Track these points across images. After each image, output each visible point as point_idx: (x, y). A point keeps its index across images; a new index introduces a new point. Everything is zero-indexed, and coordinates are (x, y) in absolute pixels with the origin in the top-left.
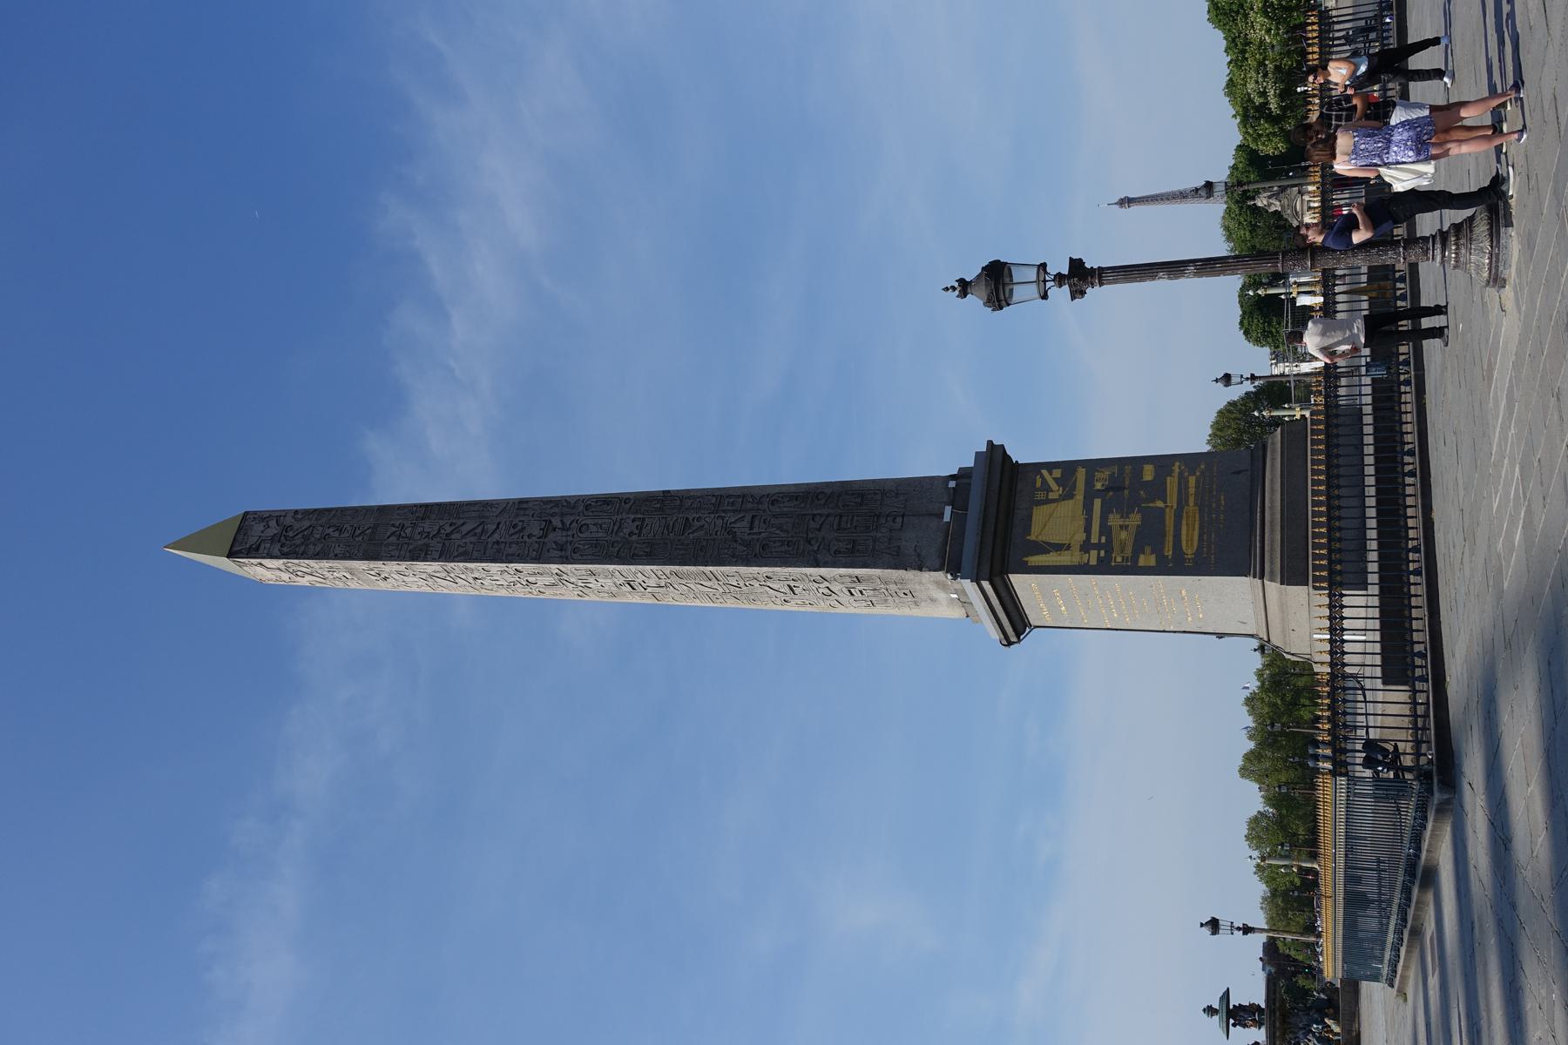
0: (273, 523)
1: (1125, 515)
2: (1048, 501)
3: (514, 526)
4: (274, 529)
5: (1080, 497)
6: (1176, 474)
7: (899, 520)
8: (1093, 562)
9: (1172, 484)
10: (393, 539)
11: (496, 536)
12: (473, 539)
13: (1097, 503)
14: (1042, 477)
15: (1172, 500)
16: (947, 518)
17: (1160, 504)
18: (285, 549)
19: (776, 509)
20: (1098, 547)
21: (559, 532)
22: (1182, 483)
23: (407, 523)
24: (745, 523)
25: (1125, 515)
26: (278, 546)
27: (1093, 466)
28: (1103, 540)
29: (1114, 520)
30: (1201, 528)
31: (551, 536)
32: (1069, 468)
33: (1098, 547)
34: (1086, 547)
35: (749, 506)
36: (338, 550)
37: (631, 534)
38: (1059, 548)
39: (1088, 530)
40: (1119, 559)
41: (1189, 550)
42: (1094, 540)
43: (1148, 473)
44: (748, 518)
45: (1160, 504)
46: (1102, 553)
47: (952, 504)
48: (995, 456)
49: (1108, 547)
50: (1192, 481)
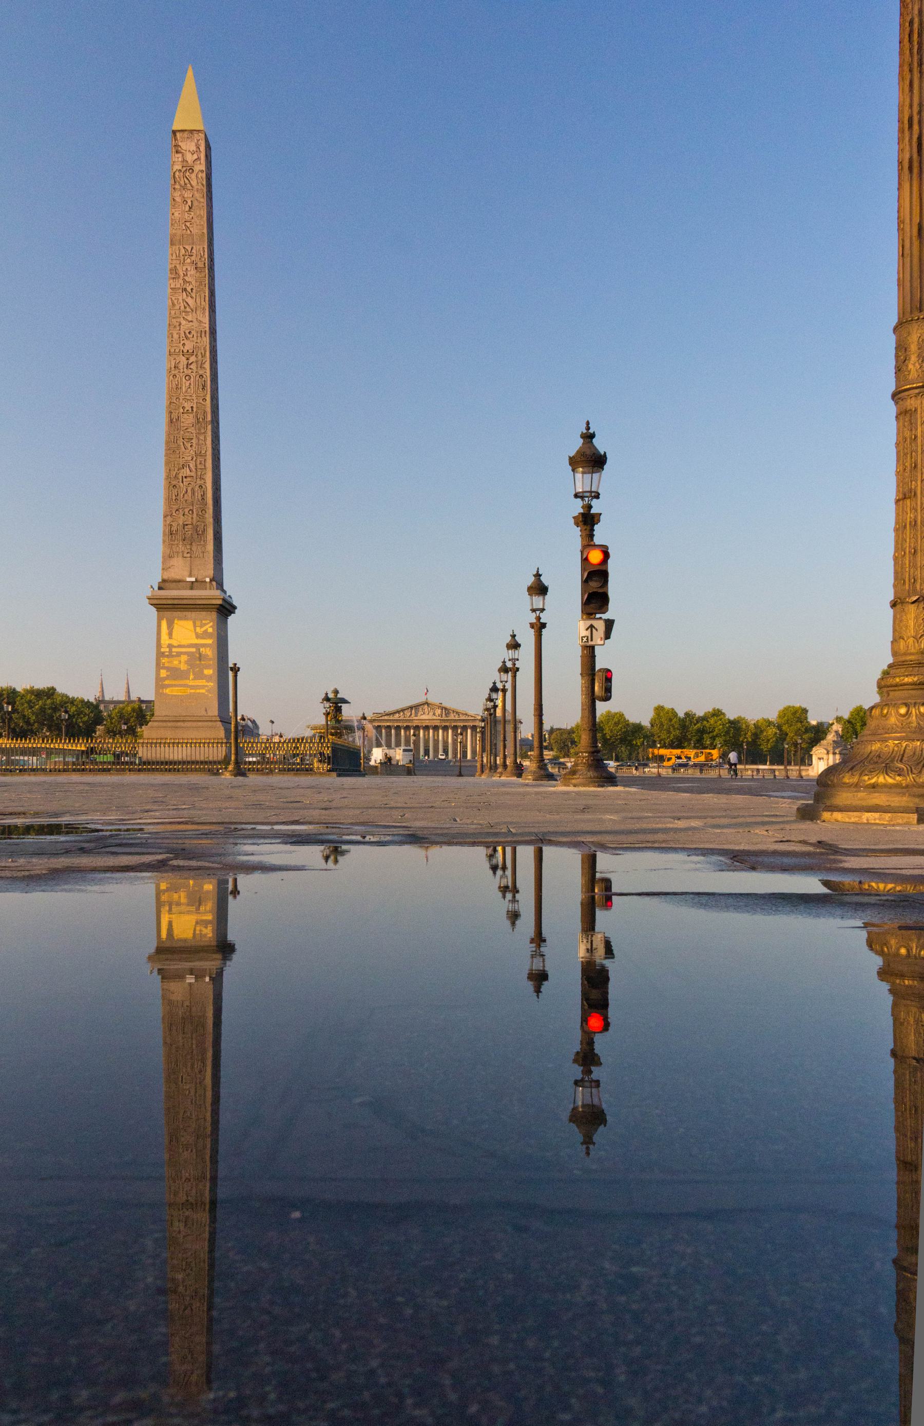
0: (195, 157)
1: (186, 662)
2: (195, 626)
3: (190, 333)
4: (190, 158)
8: (162, 650)
9: (202, 682)
10: (183, 251)
11: (183, 322)
12: (182, 308)
13: (194, 650)
16: (189, 579)
17: (192, 677)
18: (177, 173)
19: (197, 488)
20: (170, 651)
21: (186, 362)
22: (203, 687)
23: (193, 258)
24: (189, 473)
25: (186, 662)
26: (180, 167)
31: (184, 359)
33: (170, 651)
34: (170, 646)
35: (199, 473)
36: (176, 214)
37: (183, 408)
38: (170, 635)
39: (179, 646)
41: (167, 691)
42: (174, 650)
44: (193, 474)
45: (192, 677)
47: (196, 581)
49: (170, 655)
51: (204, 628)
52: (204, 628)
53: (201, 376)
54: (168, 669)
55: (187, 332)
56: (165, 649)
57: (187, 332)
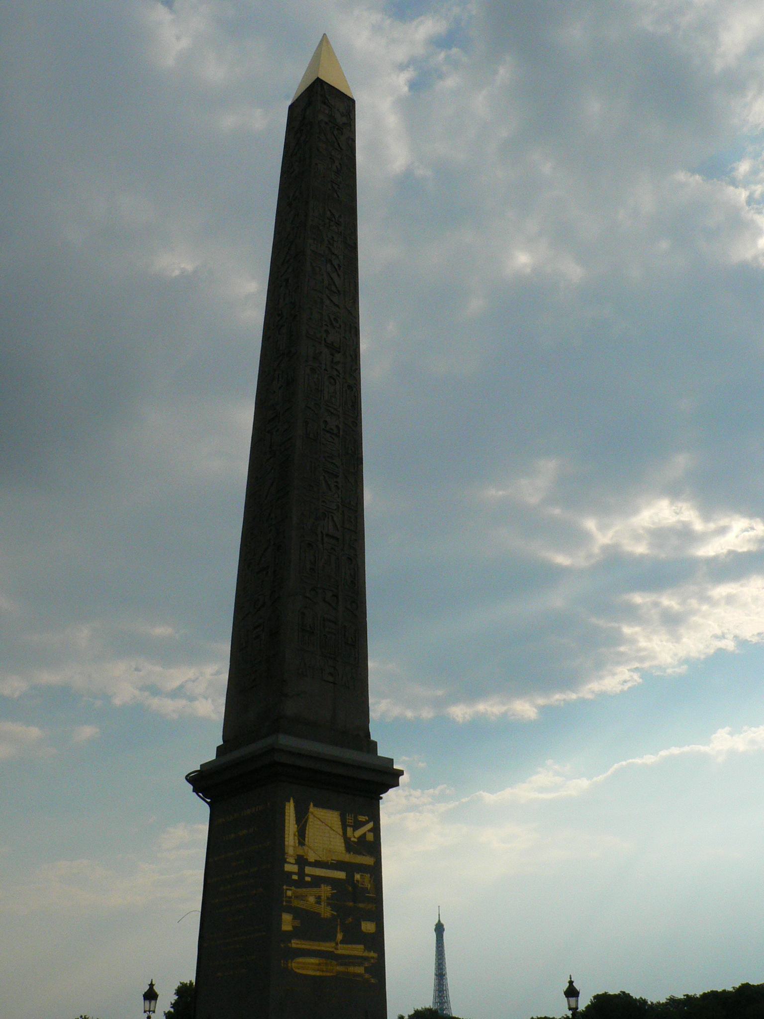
0: (344, 120)
2: (344, 826)
5: (348, 858)
6: (366, 954)
7: (331, 679)
8: (288, 868)
9: (358, 950)
11: (327, 302)
13: (341, 875)
14: (367, 822)
15: (344, 950)
17: (340, 936)
20: (301, 873)
26: (326, 120)
27: (376, 871)
28: (308, 879)
29: (326, 891)
30: (314, 977)
32: (373, 848)
33: (301, 873)
34: (301, 861)
38: (301, 834)
39: (318, 864)
40: (289, 893)
42: (308, 870)
43: (368, 927)
45: (340, 936)
46: (295, 877)
48: (389, 777)
50: (360, 970)
51: (359, 833)
52: (359, 833)
53: (350, 387)
54: (297, 913)
55: (332, 317)
56: (291, 867)
57: (332, 317)
